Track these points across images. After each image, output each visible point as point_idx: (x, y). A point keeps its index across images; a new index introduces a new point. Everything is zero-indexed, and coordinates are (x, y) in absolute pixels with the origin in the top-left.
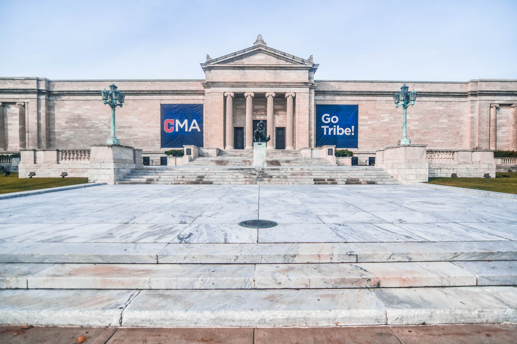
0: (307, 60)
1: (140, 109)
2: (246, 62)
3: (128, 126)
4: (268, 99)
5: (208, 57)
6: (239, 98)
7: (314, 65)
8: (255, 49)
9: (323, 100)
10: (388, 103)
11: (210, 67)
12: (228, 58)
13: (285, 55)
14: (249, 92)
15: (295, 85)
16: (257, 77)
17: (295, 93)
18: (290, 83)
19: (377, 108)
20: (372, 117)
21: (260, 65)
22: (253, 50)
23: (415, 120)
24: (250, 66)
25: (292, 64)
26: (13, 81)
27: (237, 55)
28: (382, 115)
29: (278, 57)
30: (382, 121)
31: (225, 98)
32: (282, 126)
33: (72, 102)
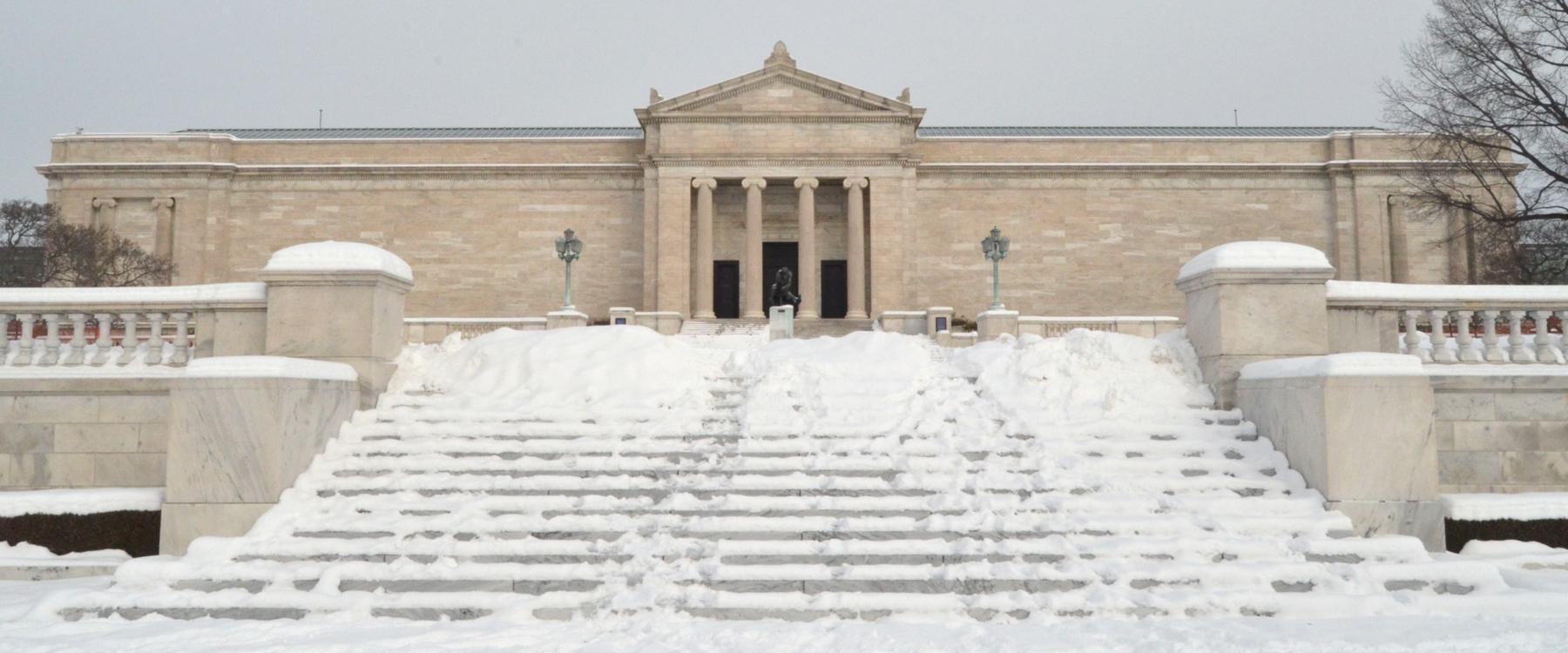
0: (894, 99)
1: (469, 214)
2: (747, 103)
3: (435, 260)
4: (802, 195)
5: (654, 94)
6: (729, 190)
7: (911, 110)
8: (769, 75)
9: (946, 189)
11: (659, 118)
12: (702, 97)
13: (840, 88)
14: (754, 177)
15: (866, 161)
17: (867, 178)
18: (855, 154)
19: (1088, 209)
22: (764, 77)
24: (756, 114)
25: (858, 109)
26: (148, 145)
27: (725, 90)
28: (1102, 227)
29: (825, 93)
30: (1103, 241)
31: (695, 192)
32: (836, 257)
33: (291, 197)
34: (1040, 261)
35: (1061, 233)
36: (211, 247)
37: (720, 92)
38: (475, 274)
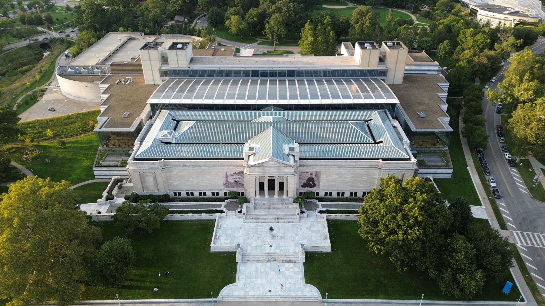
23: (350, 177)
31: (255, 179)
32: (282, 181)
33: (177, 170)
35: (325, 176)
36: (164, 180)
38: (215, 182)
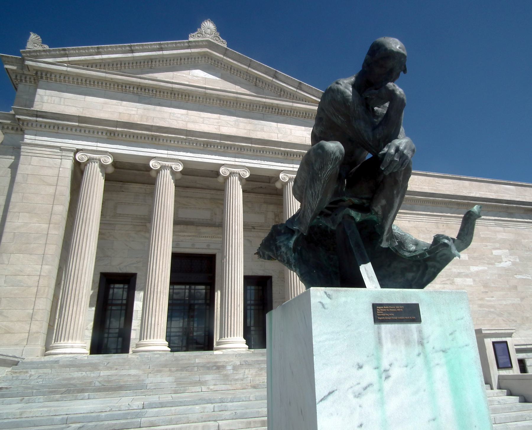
10: (501, 226)
16: (194, 122)
19: (482, 236)
20: (476, 255)
21: (205, 88)
28: (495, 252)
34: (453, 283)
37: (130, 55)
